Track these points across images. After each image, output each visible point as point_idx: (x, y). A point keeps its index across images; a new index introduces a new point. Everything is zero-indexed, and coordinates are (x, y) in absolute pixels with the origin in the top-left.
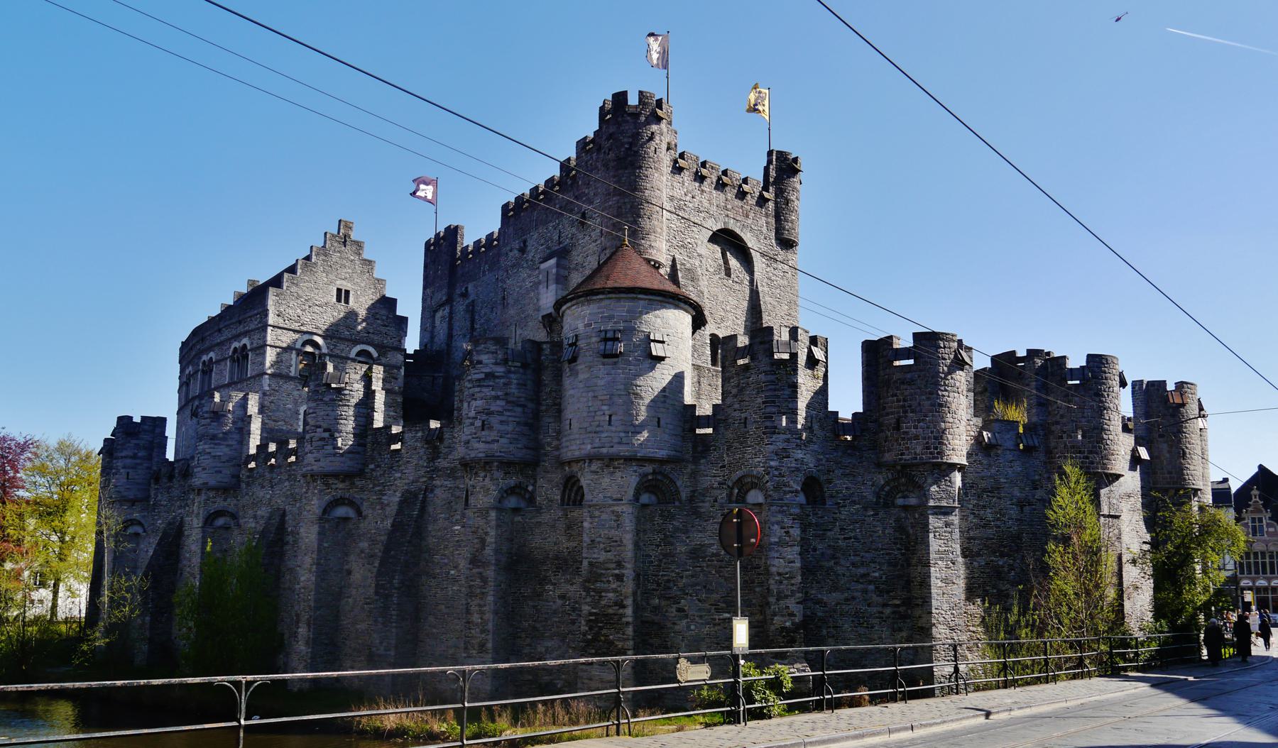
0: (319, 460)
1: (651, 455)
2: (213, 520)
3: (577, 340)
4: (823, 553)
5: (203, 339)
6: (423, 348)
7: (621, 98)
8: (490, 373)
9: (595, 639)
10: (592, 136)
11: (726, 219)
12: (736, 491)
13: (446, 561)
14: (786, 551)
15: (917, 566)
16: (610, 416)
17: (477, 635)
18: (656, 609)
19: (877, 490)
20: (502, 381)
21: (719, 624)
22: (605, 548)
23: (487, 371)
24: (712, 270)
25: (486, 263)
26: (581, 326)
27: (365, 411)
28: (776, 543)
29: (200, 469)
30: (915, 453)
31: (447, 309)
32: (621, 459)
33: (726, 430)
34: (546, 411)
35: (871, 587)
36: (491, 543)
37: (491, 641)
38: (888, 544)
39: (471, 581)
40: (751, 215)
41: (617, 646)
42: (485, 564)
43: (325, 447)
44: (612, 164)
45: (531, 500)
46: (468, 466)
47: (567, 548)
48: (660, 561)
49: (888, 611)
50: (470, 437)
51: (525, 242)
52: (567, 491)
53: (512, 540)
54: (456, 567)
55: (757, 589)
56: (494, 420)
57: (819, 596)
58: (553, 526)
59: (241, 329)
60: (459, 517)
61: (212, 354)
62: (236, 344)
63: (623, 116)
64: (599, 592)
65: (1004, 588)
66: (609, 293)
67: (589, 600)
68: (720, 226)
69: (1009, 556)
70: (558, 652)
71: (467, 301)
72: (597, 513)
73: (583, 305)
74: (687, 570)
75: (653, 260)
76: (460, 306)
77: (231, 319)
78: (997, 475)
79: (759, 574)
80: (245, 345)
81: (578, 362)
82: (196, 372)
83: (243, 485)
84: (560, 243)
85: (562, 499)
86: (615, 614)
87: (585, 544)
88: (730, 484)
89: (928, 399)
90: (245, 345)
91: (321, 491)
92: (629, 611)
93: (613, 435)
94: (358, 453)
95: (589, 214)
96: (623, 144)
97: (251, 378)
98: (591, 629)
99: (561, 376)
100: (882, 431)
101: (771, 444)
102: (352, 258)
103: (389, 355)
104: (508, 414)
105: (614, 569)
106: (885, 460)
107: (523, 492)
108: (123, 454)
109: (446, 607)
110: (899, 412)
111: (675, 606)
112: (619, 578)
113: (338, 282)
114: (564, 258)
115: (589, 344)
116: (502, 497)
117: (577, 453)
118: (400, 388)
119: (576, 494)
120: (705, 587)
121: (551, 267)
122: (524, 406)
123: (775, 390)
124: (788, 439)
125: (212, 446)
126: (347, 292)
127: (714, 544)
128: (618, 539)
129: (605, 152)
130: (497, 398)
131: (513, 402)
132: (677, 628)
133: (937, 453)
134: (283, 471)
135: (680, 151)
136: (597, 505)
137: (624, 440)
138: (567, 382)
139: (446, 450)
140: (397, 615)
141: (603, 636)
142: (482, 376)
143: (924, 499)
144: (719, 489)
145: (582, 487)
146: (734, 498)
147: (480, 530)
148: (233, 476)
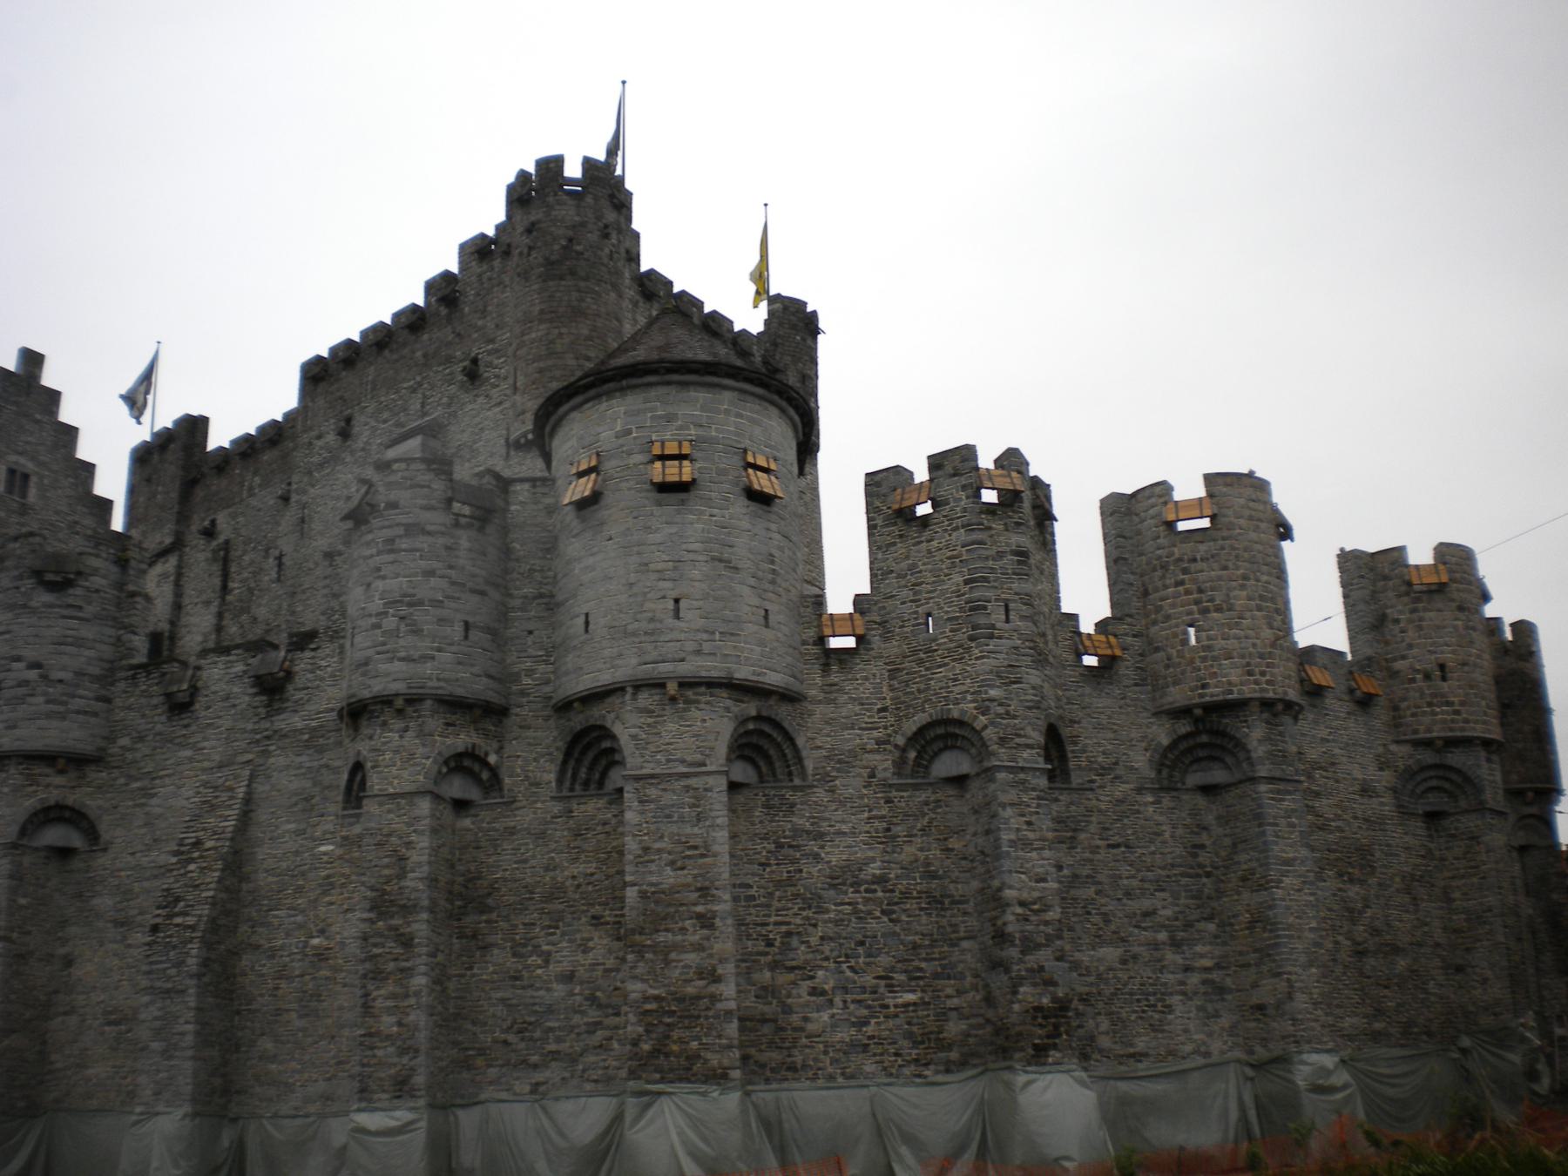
0: (14, 727)
1: (761, 679)
3: (599, 462)
4: (1075, 876)
7: (552, 165)
8: (414, 525)
9: (656, 1052)
10: (491, 232)
12: (912, 755)
13: (299, 918)
14: (1031, 859)
15: (1239, 893)
16: (677, 601)
17: (390, 1060)
18: (766, 992)
19: (1157, 756)
20: (441, 541)
21: (896, 1016)
22: (672, 863)
23: (410, 521)
25: (255, 473)
26: (607, 437)
27: (111, 632)
28: (1012, 843)
30: (1230, 683)
31: (172, 561)
32: (699, 684)
33: (886, 640)
34: (523, 609)
35: (1162, 936)
36: (420, 864)
37: (422, 1070)
38: (1181, 857)
39: (375, 945)
41: (706, 1061)
42: (408, 910)
43: (30, 699)
45: (492, 782)
46: (356, 713)
47: (574, 877)
48: (771, 894)
49: (1194, 979)
51: (349, 420)
52: (572, 763)
53: (452, 866)
54: (322, 932)
55: (965, 944)
57: (1077, 954)
58: (542, 835)
60: (330, 827)
63: (556, 195)
64: (664, 952)
65: (1360, 939)
66: (669, 371)
67: (641, 969)
69: (1362, 882)
72: (653, 792)
73: (609, 394)
74: (827, 911)
76: (199, 556)
78: (1328, 741)
79: (965, 913)
81: (603, 503)
84: (425, 414)
85: (560, 781)
86: (699, 998)
87: (631, 857)
88: (901, 741)
89: (1243, 587)
92: (728, 989)
93: (682, 636)
94: (95, 714)
98: (647, 1031)
99: (556, 538)
100: (1157, 649)
101: (988, 658)
102: (38, 416)
104: (453, 605)
105: (695, 905)
106: (1170, 699)
107: (476, 767)
109: (301, 1017)
110: (1190, 613)
111: (806, 985)
112: (706, 921)
113: (13, 458)
114: (434, 437)
115: (627, 467)
116: (439, 772)
117: (605, 678)
119: (591, 769)
120: (862, 943)
122: (482, 593)
123: (987, 558)
124: (1016, 648)
126: (26, 477)
127: (873, 859)
128: (698, 841)
129: (521, 254)
130: (430, 573)
131: (464, 585)
132: (810, 1027)
133: (1269, 682)
135: (644, 268)
136: (652, 776)
137: (707, 647)
138: (572, 547)
139: (299, 695)
140: (197, 1033)
141: (675, 1042)
142: (401, 531)
143: (1245, 765)
144: (877, 751)
145: (612, 751)
146: (908, 769)
147: (393, 839)
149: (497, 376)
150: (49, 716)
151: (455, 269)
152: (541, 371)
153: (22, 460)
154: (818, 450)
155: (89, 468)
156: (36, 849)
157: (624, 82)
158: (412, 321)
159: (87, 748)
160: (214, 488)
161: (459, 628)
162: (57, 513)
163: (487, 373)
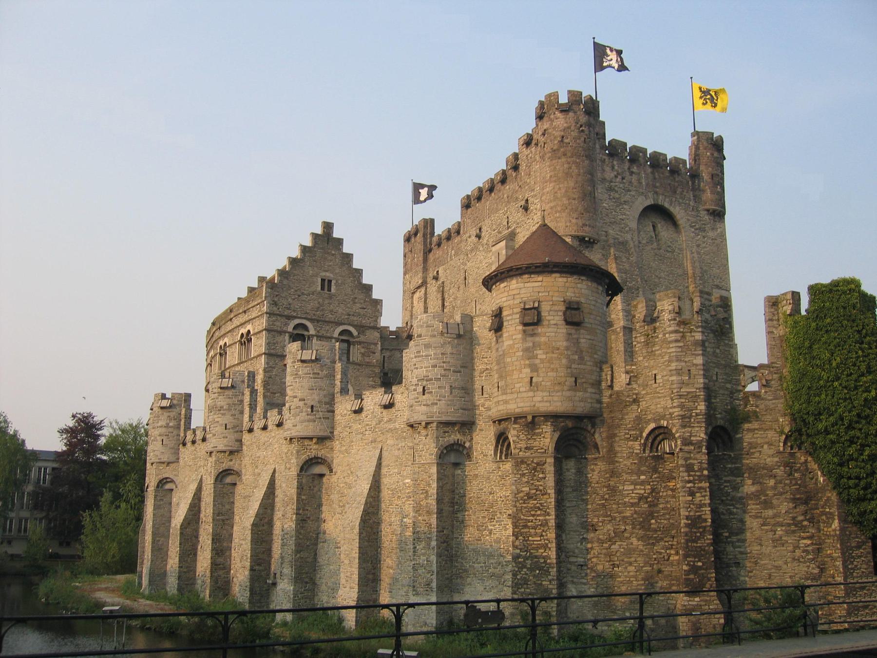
2: (223, 477)
5: (219, 328)
6: (405, 325)
11: (655, 195)
24: (644, 242)
25: (452, 249)
29: (211, 435)
31: (423, 290)
37: (435, 580)
40: (679, 190)
44: (548, 155)
50: (414, 401)
51: (480, 229)
53: (454, 491)
56: (432, 387)
58: (488, 478)
59: (246, 317)
61: (226, 340)
62: (244, 331)
63: (555, 114)
68: (649, 202)
70: (495, 591)
71: (440, 282)
75: (587, 237)
77: (238, 310)
80: (249, 332)
81: (504, 330)
82: (215, 355)
83: (244, 448)
85: (496, 454)
90: (249, 332)
91: (298, 452)
94: (328, 418)
95: (531, 200)
96: (555, 138)
97: (254, 358)
102: (333, 252)
103: (368, 332)
107: (461, 449)
108: (159, 424)
113: (324, 274)
114: (512, 240)
116: (442, 452)
118: (377, 361)
121: (501, 249)
122: (460, 372)
125: (220, 415)
126: (330, 282)
130: (434, 366)
134: (273, 435)
137: (545, 399)
140: (359, 558)
148: (237, 441)
149: (536, 209)
150: (308, 421)
151: (517, 151)
152: (551, 208)
153: (328, 274)
154: (724, 214)
155: (359, 272)
156: (308, 476)
157: (594, 38)
158: (504, 179)
159: (325, 434)
160: (437, 256)
161: (448, 389)
162: (346, 295)
163: (532, 207)
